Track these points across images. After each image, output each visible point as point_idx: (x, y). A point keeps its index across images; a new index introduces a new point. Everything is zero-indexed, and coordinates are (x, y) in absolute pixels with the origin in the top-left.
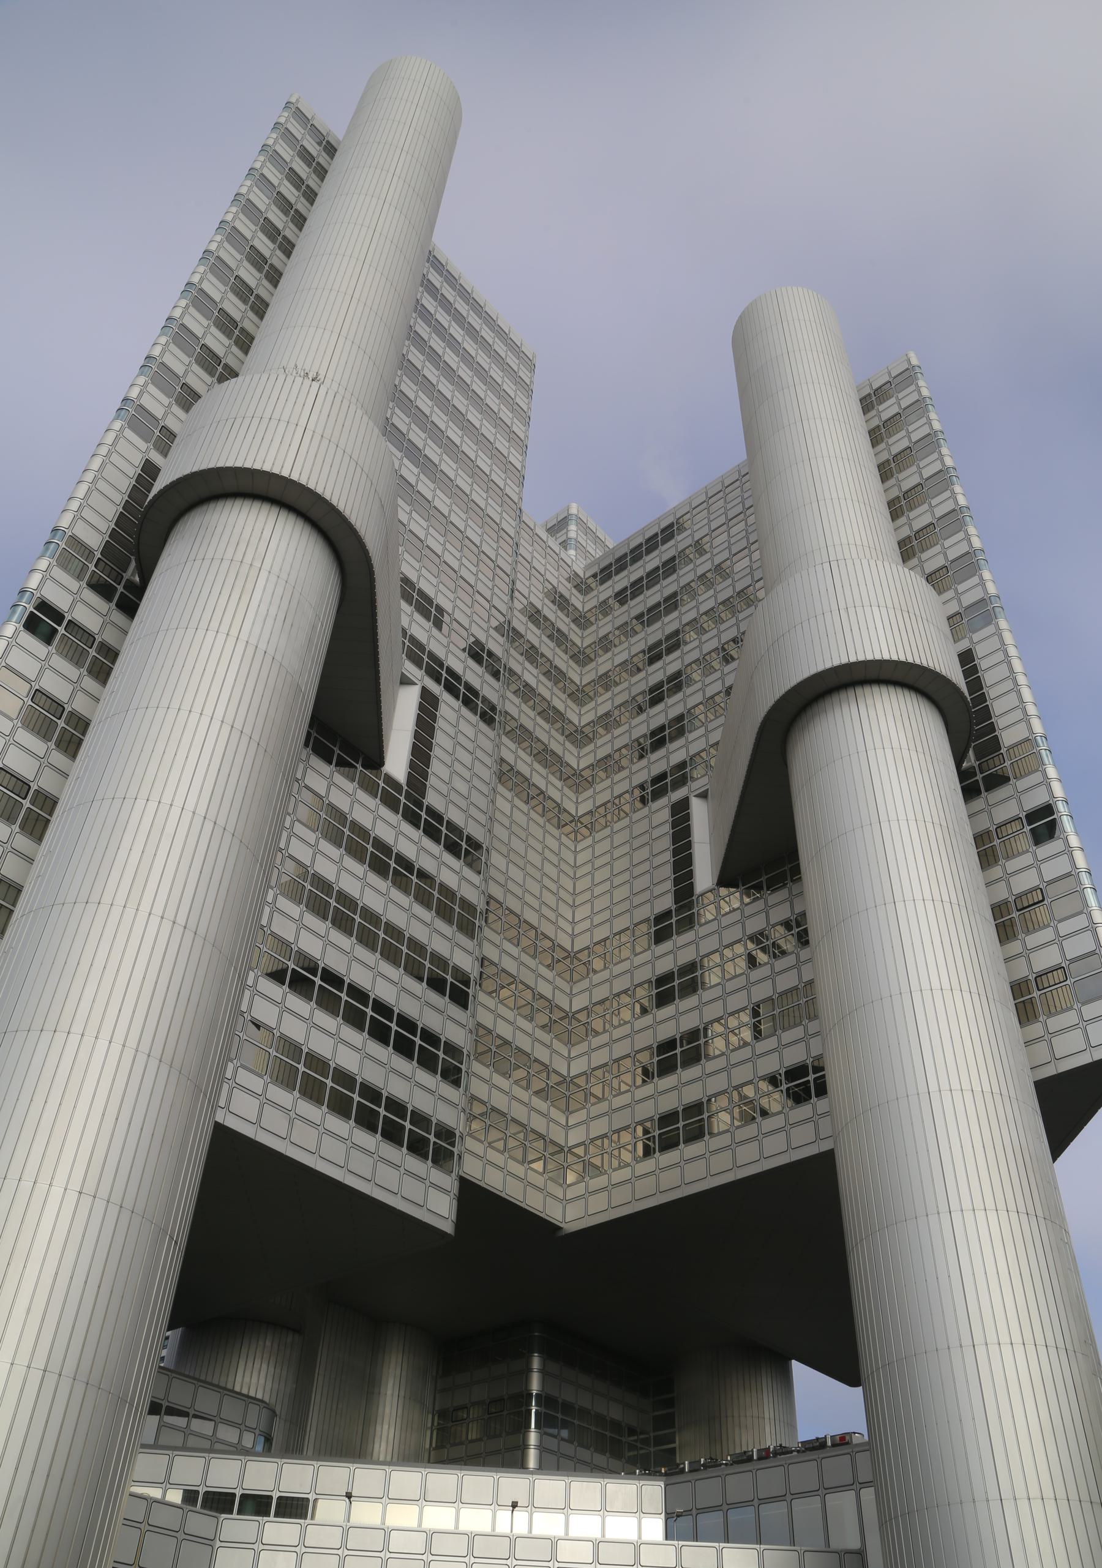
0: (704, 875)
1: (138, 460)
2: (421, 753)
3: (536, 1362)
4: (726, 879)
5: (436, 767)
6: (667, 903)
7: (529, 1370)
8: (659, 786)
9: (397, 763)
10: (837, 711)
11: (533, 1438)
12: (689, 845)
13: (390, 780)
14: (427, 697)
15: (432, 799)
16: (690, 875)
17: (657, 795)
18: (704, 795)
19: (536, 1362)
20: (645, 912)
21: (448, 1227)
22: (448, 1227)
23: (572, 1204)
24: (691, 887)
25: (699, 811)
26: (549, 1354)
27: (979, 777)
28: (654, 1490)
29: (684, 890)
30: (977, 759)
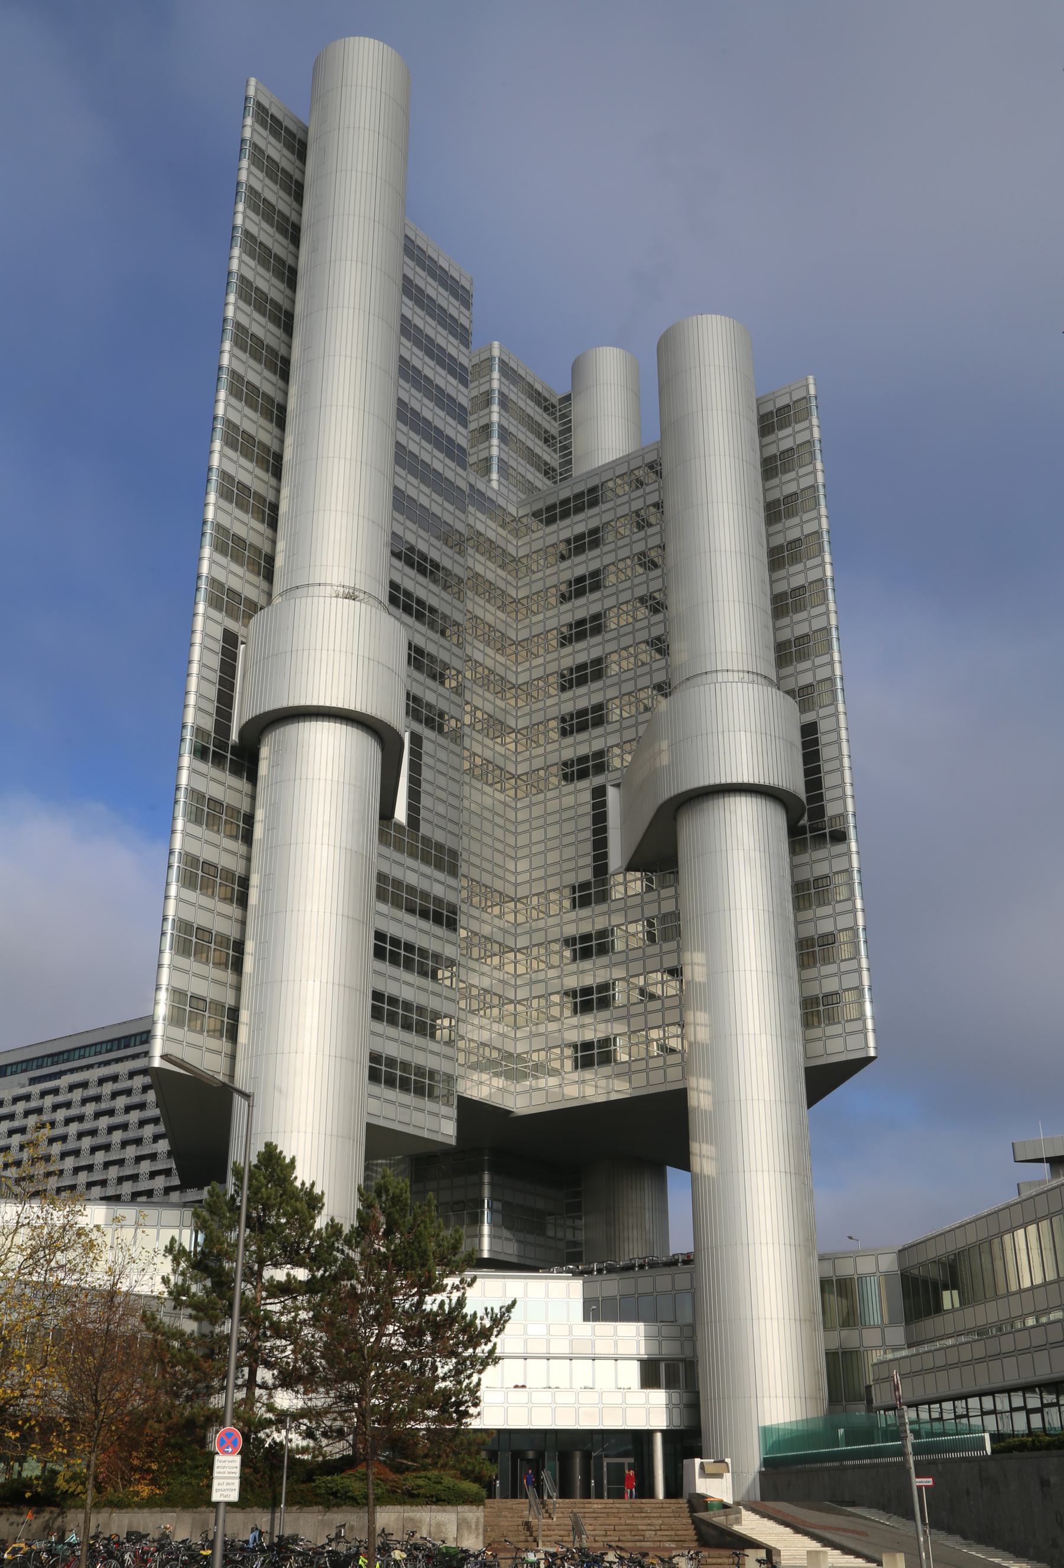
0: (616, 859)
1: (219, 634)
2: (414, 795)
3: (486, 1178)
4: (631, 867)
5: (425, 801)
6: (587, 875)
7: (482, 1183)
9: (401, 814)
12: (604, 830)
13: (399, 827)
15: (425, 829)
16: (605, 856)
17: (583, 774)
18: (617, 786)
19: (486, 1178)
21: (453, 1142)
22: (453, 1142)
23: (522, 1098)
24: (605, 866)
25: (613, 795)
26: (494, 1171)
27: (808, 835)
29: (601, 869)
30: (809, 820)
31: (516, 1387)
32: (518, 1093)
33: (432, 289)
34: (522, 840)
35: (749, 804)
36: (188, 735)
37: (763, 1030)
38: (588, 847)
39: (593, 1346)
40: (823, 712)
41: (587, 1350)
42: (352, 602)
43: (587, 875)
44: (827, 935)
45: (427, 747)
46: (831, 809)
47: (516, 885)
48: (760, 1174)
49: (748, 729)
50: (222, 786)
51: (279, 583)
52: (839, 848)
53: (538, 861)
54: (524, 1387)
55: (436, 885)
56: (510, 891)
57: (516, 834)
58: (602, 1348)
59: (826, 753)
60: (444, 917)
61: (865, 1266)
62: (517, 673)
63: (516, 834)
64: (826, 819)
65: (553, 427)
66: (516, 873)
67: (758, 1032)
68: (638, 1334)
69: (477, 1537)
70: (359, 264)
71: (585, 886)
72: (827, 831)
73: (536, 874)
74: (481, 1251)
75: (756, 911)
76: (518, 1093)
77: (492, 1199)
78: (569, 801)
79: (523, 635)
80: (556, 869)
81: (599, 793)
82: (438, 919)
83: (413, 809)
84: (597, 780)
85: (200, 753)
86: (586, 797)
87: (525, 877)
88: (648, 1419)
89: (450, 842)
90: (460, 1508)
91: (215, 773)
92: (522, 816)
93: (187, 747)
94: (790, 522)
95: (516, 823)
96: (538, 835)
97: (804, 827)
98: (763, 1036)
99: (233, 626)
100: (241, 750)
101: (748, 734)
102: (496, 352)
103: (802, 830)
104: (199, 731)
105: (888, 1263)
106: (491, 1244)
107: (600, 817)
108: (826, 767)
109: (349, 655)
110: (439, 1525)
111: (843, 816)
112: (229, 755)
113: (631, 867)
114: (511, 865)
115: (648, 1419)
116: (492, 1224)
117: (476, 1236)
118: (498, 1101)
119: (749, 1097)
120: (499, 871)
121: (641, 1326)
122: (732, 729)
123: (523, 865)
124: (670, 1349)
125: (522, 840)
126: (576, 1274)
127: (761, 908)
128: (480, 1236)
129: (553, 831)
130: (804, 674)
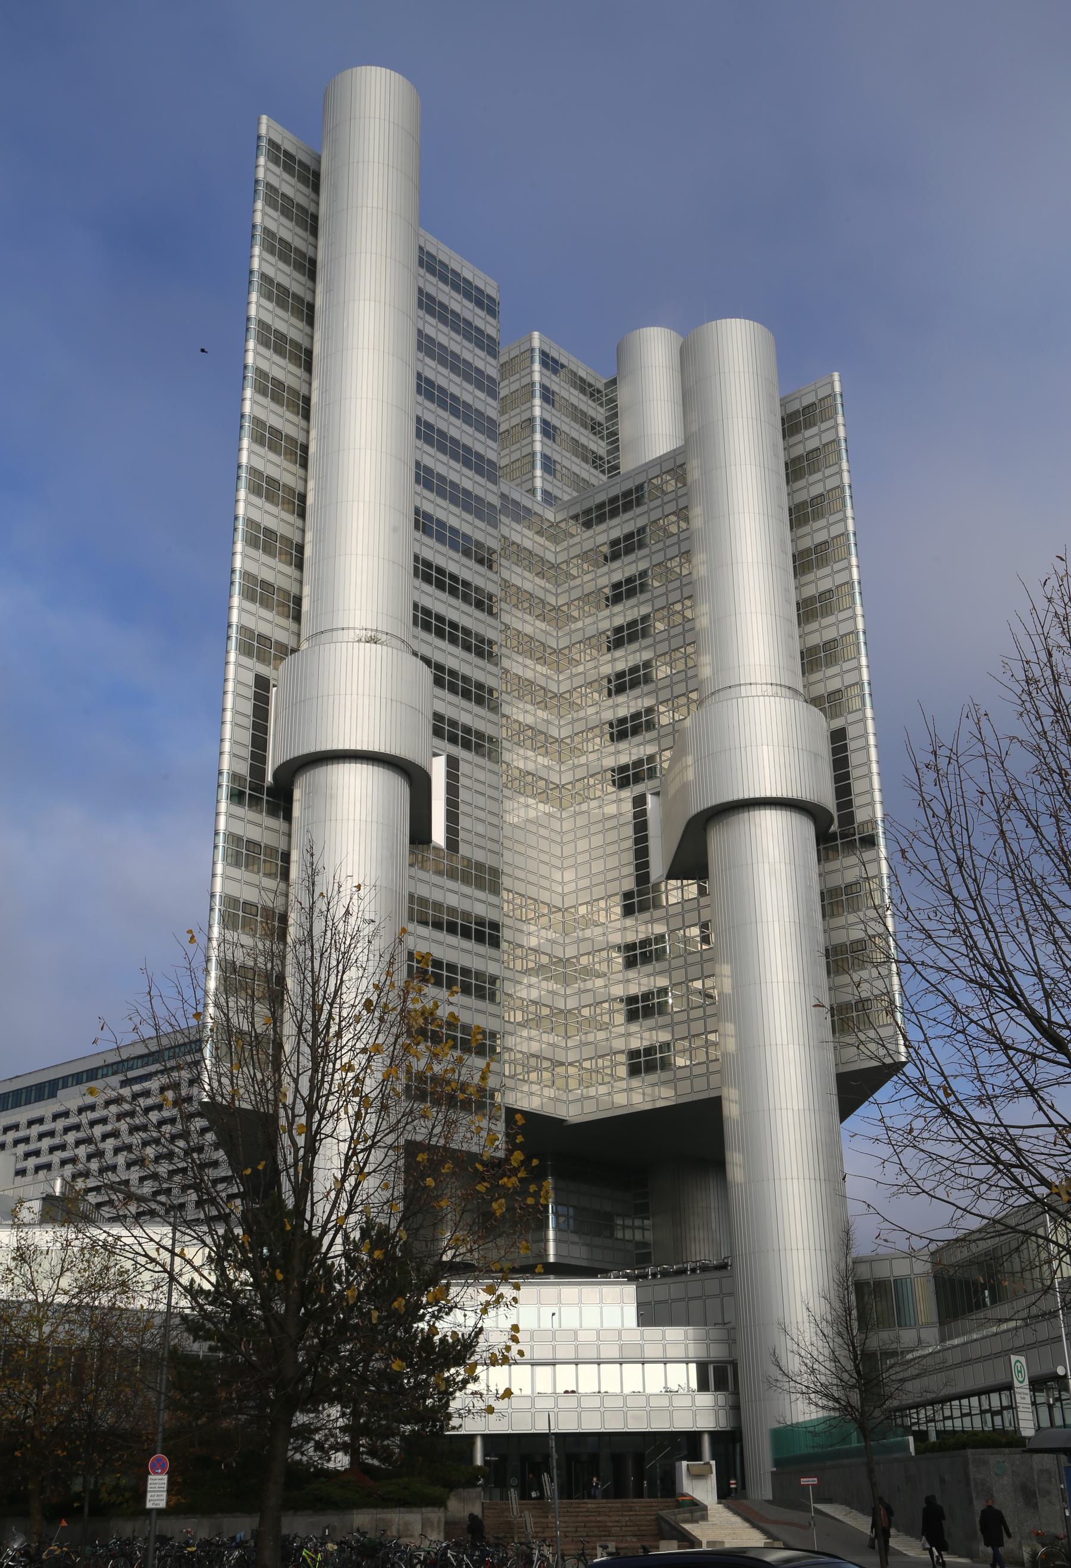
0: (657, 868)
1: (250, 679)
2: (452, 817)
5: (464, 822)
6: (629, 884)
8: (625, 776)
9: (439, 835)
10: (741, 815)
11: (551, 1234)
12: (645, 839)
13: (437, 849)
14: (452, 763)
15: (464, 850)
16: (646, 865)
18: (657, 794)
20: (614, 887)
26: (558, 1176)
27: (839, 842)
28: (631, 1290)
30: (839, 827)
31: (566, 1392)
32: (571, 1102)
33: (457, 303)
34: (568, 850)
35: (774, 816)
36: (225, 781)
37: (791, 1040)
38: (629, 857)
39: (643, 1351)
40: (851, 718)
41: (636, 1354)
42: (374, 645)
43: (629, 884)
44: (858, 941)
45: (464, 768)
46: (861, 816)
47: (563, 895)
48: (789, 1181)
49: (770, 742)
50: (258, 826)
51: (306, 629)
52: (868, 855)
53: (583, 871)
54: (573, 1392)
55: (476, 903)
56: (557, 901)
57: (562, 844)
58: (650, 1352)
59: (854, 759)
60: (487, 933)
61: (901, 1269)
62: (559, 682)
63: (562, 844)
64: (856, 825)
65: (599, 413)
66: (563, 883)
67: (785, 1042)
68: (686, 1338)
69: (439, 1534)
70: (372, 303)
71: (628, 895)
72: (857, 837)
73: (583, 883)
74: (547, 1255)
75: (782, 923)
76: (571, 1102)
77: (556, 1203)
78: (611, 809)
79: (564, 643)
80: (600, 879)
81: (639, 801)
82: (480, 938)
83: (452, 831)
84: (638, 789)
85: (237, 796)
86: (628, 807)
87: (571, 887)
88: (695, 1422)
89: (489, 860)
90: (424, 1510)
91: (252, 815)
92: (567, 825)
93: (224, 792)
94: (818, 524)
95: (562, 833)
96: (583, 845)
97: (835, 833)
98: (791, 1046)
99: (264, 670)
100: (275, 789)
101: (771, 748)
102: (536, 344)
103: (833, 837)
104: (235, 777)
105: (922, 1267)
106: (557, 1248)
107: (641, 826)
108: (854, 773)
109: (372, 698)
110: (406, 1524)
111: (873, 822)
112: (265, 797)
113: (670, 877)
114: (557, 876)
115: (695, 1422)
116: (557, 1229)
117: (542, 1241)
118: (549, 1110)
119: (778, 1106)
120: (544, 883)
121: (690, 1330)
122: (754, 744)
123: (569, 875)
124: (717, 1352)
125: (568, 850)
126: (631, 1279)
127: (787, 919)
128: (546, 1240)
129: (597, 841)
130: (830, 679)
